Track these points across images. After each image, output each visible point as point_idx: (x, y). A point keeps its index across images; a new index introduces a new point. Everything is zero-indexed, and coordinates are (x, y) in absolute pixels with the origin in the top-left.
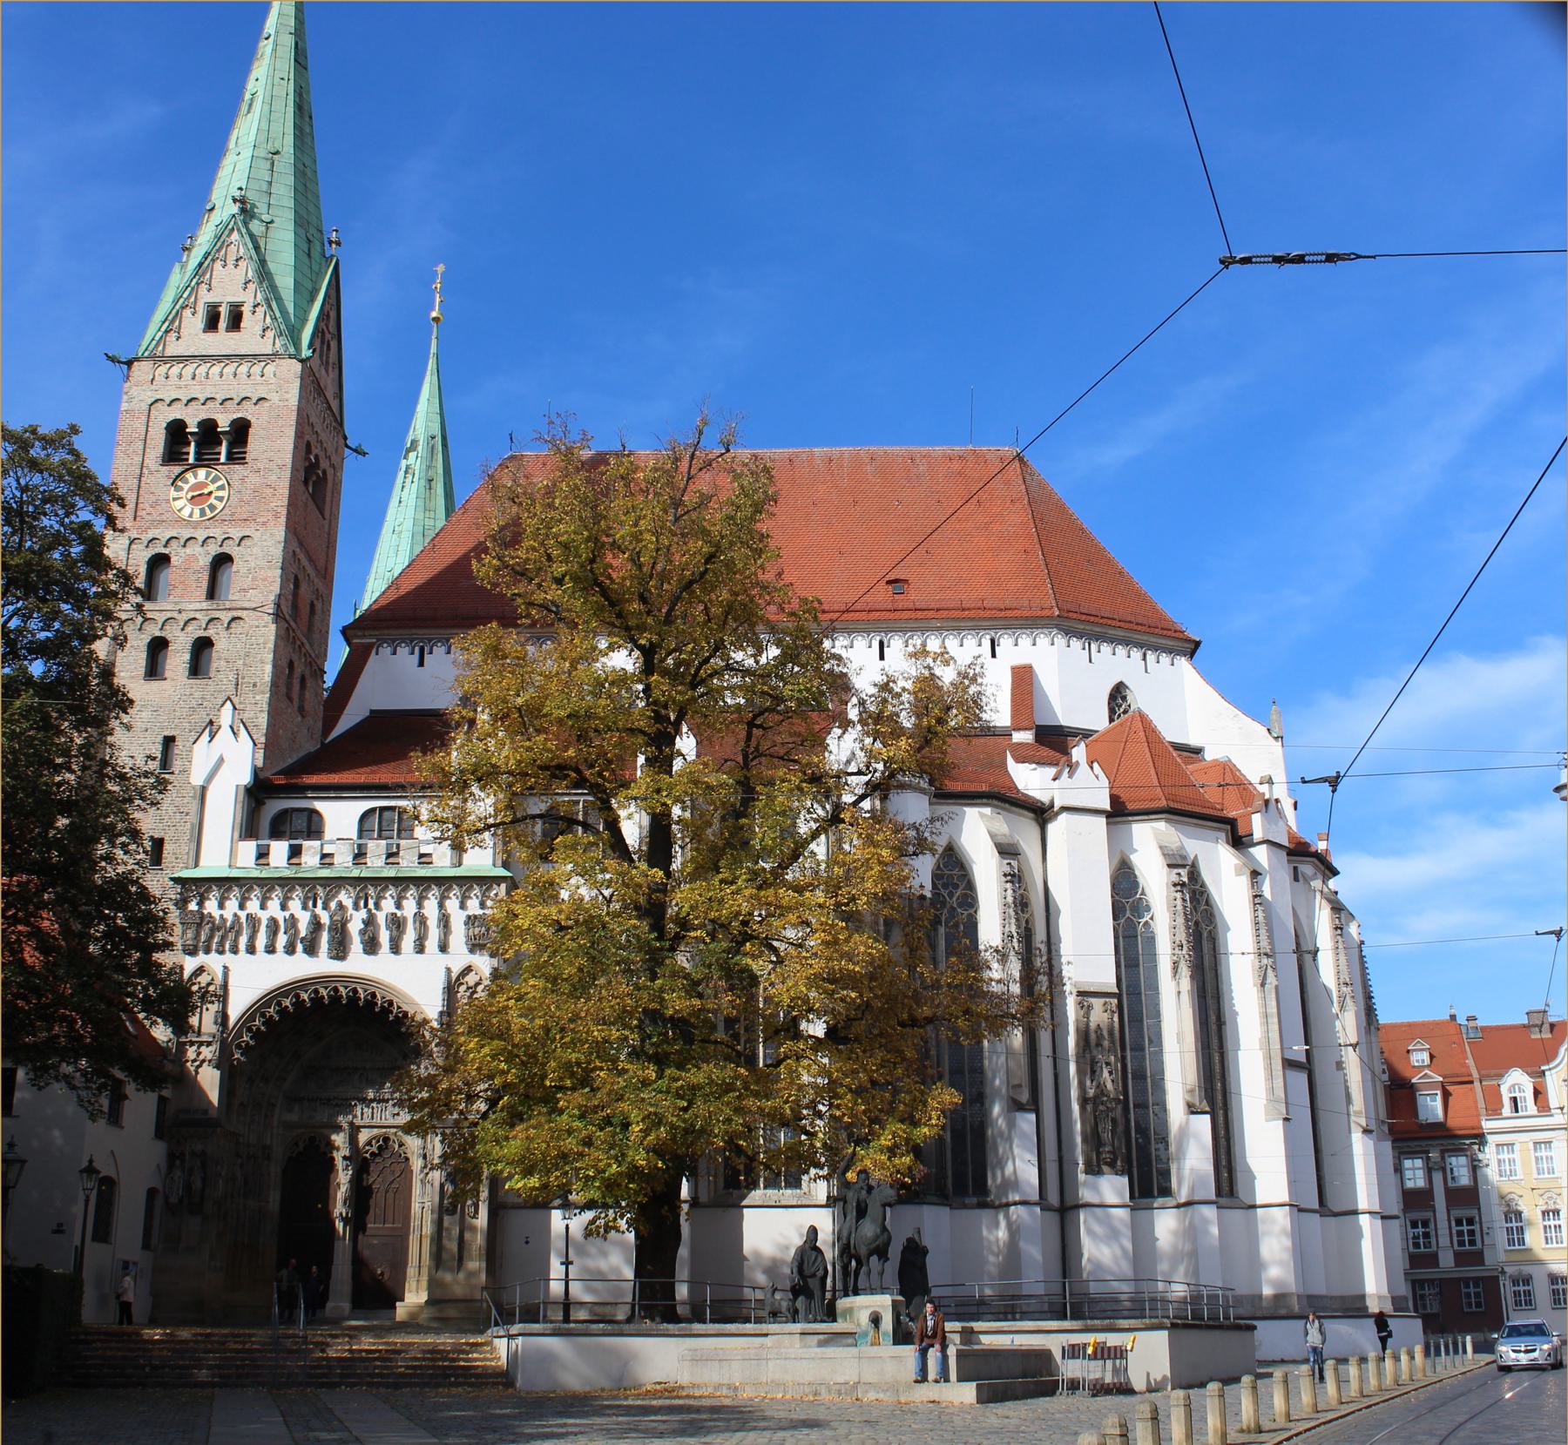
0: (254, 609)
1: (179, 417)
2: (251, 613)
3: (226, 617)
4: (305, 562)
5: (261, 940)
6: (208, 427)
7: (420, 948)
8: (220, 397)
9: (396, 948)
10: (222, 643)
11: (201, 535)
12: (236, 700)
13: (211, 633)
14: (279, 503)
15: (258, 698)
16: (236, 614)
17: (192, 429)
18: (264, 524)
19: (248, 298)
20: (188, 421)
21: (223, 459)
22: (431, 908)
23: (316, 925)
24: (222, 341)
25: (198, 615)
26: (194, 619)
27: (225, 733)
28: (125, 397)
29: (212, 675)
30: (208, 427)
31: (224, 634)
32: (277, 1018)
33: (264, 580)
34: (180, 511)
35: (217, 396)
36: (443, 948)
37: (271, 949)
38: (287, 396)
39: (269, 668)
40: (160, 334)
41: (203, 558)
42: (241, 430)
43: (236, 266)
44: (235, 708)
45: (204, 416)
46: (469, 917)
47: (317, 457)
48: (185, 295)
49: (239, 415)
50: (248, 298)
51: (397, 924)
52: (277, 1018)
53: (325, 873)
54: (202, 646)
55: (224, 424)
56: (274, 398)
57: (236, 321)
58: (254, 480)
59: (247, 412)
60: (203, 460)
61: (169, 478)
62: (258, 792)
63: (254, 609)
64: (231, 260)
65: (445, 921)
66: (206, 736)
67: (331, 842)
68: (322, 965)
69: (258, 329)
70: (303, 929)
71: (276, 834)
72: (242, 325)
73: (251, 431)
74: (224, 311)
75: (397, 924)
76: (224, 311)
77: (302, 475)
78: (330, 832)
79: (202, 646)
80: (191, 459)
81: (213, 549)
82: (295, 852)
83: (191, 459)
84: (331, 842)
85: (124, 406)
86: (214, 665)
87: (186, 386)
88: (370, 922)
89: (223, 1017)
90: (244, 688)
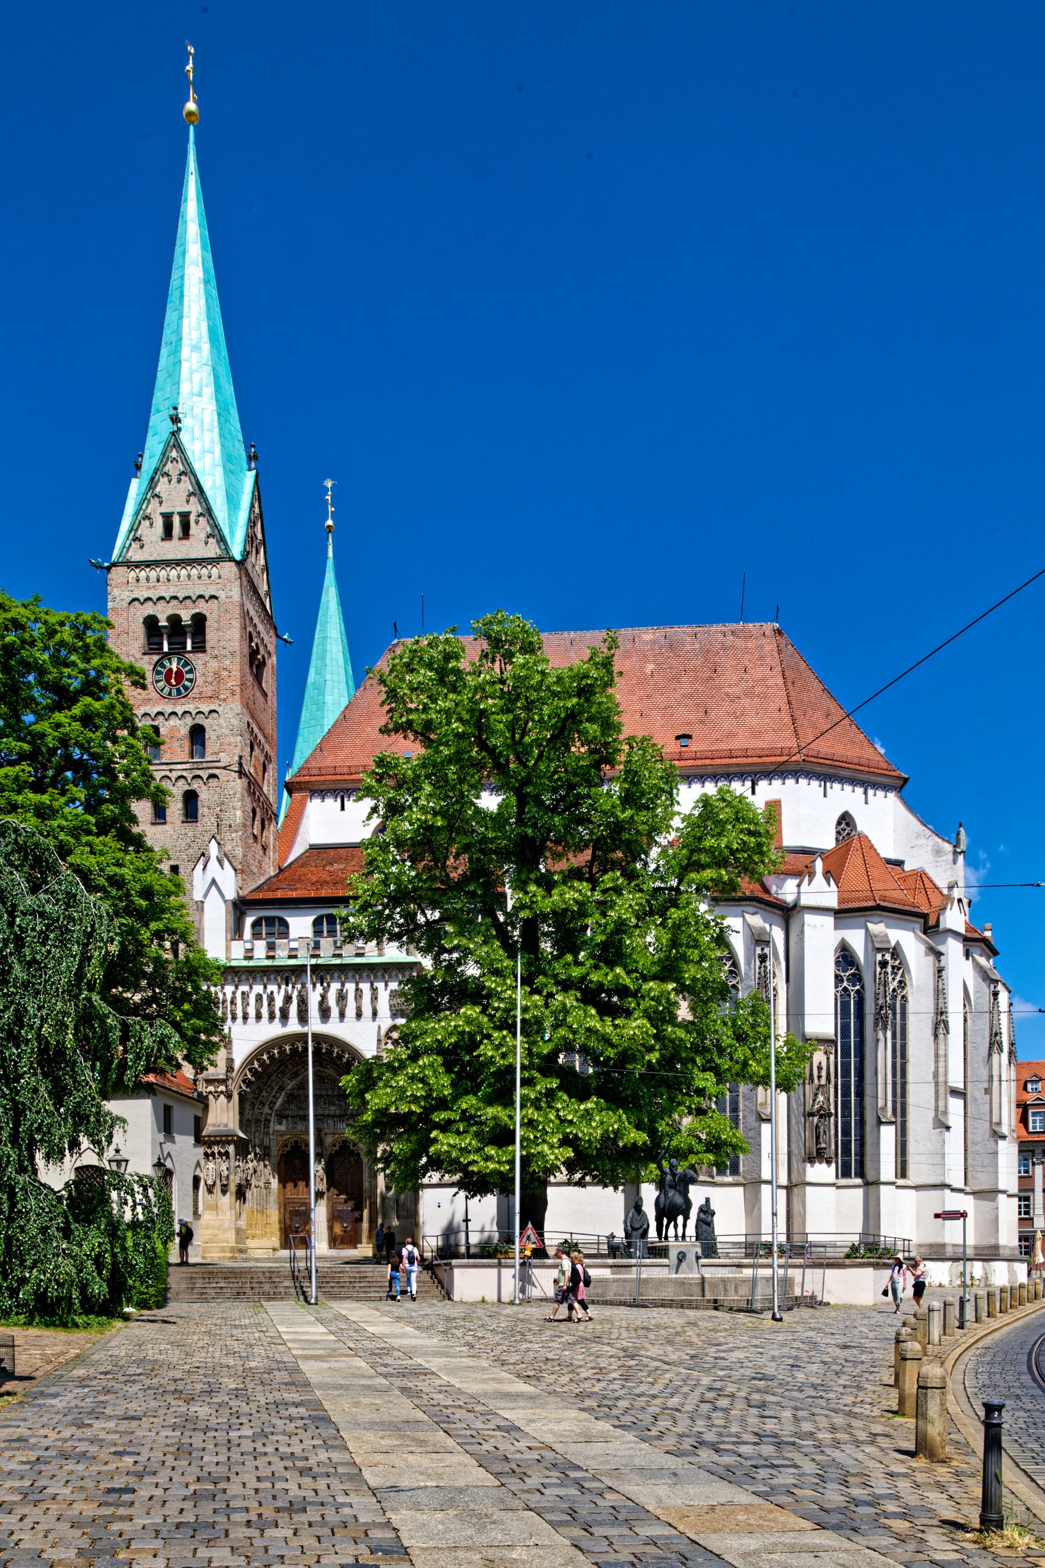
0: (224, 768)
1: (152, 613)
2: (222, 771)
3: (204, 774)
4: (256, 730)
5: (252, 1011)
6: (175, 620)
7: (359, 1015)
8: (181, 596)
9: (342, 1015)
10: (205, 795)
11: (180, 710)
12: (218, 837)
13: (196, 785)
14: (234, 683)
15: (234, 835)
16: (211, 771)
17: (163, 623)
18: (224, 700)
19: (194, 507)
20: (159, 616)
21: (189, 647)
22: (365, 987)
23: (288, 999)
24: (175, 549)
25: (185, 774)
26: (182, 777)
27: (213, 863)
28: (110, 597)
29: (199, 818)
30: (175, 620)
31: (204, 788)
32: (268, 1062)
33: (229, 745)
34: (162, 690)
35: (178, 595)
36: (375, 1014)
37: (259, 1017)
38: (230, 594)
39: (239, 813)
40: (128, 542)
41: (183, 727)
42: (199, 621)
43: (179, 481)
44: (219, 844)
45: (170, 612)
46: (392, 991)
47: (257, 644)
48: (144, 507)
49: (197, 611)
50: (194, 507)
51: (342, 997)
52: (268, 1062)
53: (292, 962)
54: (190, 798)
55: (186, 617)
56: (222, 595)
57: (186, 533)
58: (214, 664)
59: (202, 607)
60: (178, 649)
61: (150, 664)
62: (240, 907)
63: (224, 768)
64: (174, 480)
65: (374, 998)
66: (200, 866)
67: (294, 940)
68: (294, 1026)
69: (203, 536)
70: (279, 1002)
71: (256, 936)
72: (191, 532)
73: (208, 624)
74: (176, 521)
75: (342, 997)
76: (176, 521)
77: (247, 660)
78: (293, 933)
79: (190, 798)
80: (166, 648)
81: (189, 721)
82: (271, 947)
83: (166, 648)
84: (294, 940)
85: (110, 605)
86: (200, 812)
87: (154, 587)
88: (324, 997)
89: (230, 1061)
90: (224, 829)
